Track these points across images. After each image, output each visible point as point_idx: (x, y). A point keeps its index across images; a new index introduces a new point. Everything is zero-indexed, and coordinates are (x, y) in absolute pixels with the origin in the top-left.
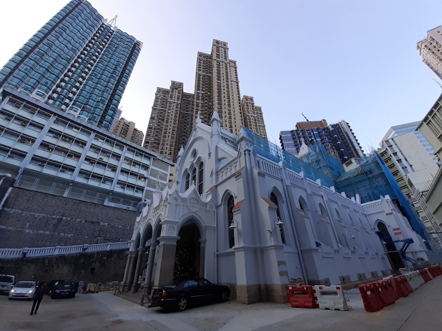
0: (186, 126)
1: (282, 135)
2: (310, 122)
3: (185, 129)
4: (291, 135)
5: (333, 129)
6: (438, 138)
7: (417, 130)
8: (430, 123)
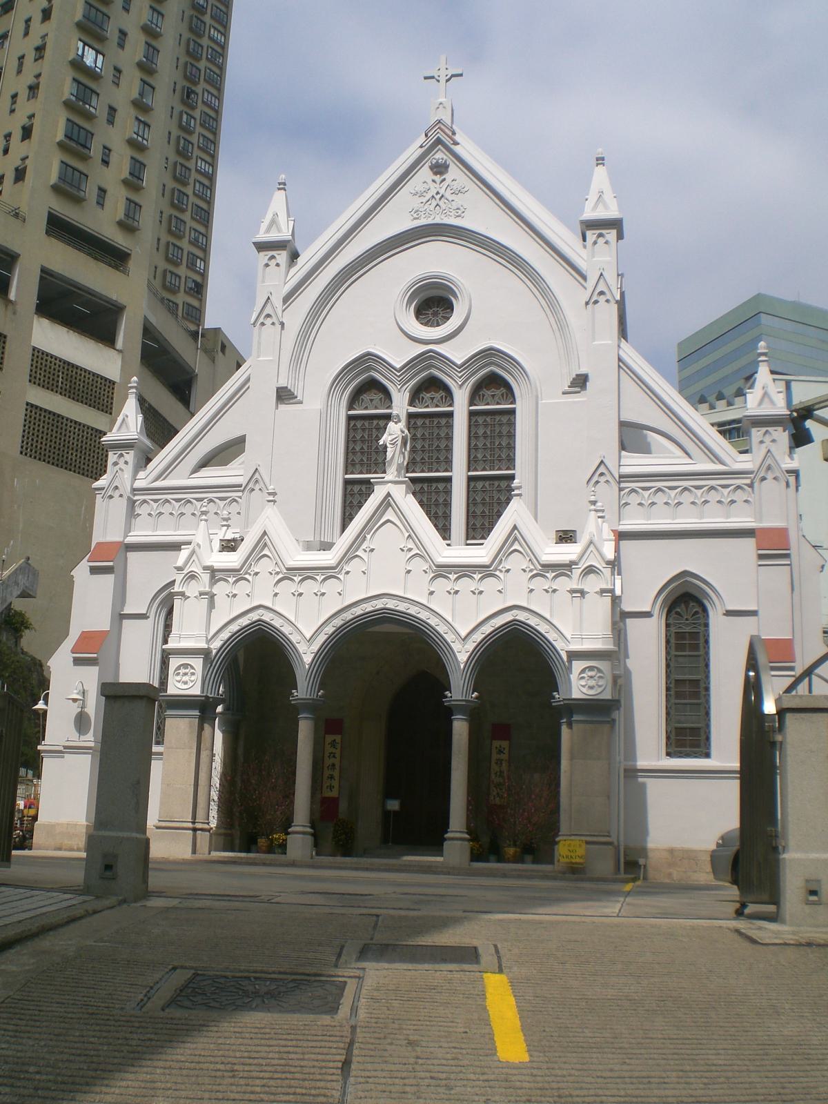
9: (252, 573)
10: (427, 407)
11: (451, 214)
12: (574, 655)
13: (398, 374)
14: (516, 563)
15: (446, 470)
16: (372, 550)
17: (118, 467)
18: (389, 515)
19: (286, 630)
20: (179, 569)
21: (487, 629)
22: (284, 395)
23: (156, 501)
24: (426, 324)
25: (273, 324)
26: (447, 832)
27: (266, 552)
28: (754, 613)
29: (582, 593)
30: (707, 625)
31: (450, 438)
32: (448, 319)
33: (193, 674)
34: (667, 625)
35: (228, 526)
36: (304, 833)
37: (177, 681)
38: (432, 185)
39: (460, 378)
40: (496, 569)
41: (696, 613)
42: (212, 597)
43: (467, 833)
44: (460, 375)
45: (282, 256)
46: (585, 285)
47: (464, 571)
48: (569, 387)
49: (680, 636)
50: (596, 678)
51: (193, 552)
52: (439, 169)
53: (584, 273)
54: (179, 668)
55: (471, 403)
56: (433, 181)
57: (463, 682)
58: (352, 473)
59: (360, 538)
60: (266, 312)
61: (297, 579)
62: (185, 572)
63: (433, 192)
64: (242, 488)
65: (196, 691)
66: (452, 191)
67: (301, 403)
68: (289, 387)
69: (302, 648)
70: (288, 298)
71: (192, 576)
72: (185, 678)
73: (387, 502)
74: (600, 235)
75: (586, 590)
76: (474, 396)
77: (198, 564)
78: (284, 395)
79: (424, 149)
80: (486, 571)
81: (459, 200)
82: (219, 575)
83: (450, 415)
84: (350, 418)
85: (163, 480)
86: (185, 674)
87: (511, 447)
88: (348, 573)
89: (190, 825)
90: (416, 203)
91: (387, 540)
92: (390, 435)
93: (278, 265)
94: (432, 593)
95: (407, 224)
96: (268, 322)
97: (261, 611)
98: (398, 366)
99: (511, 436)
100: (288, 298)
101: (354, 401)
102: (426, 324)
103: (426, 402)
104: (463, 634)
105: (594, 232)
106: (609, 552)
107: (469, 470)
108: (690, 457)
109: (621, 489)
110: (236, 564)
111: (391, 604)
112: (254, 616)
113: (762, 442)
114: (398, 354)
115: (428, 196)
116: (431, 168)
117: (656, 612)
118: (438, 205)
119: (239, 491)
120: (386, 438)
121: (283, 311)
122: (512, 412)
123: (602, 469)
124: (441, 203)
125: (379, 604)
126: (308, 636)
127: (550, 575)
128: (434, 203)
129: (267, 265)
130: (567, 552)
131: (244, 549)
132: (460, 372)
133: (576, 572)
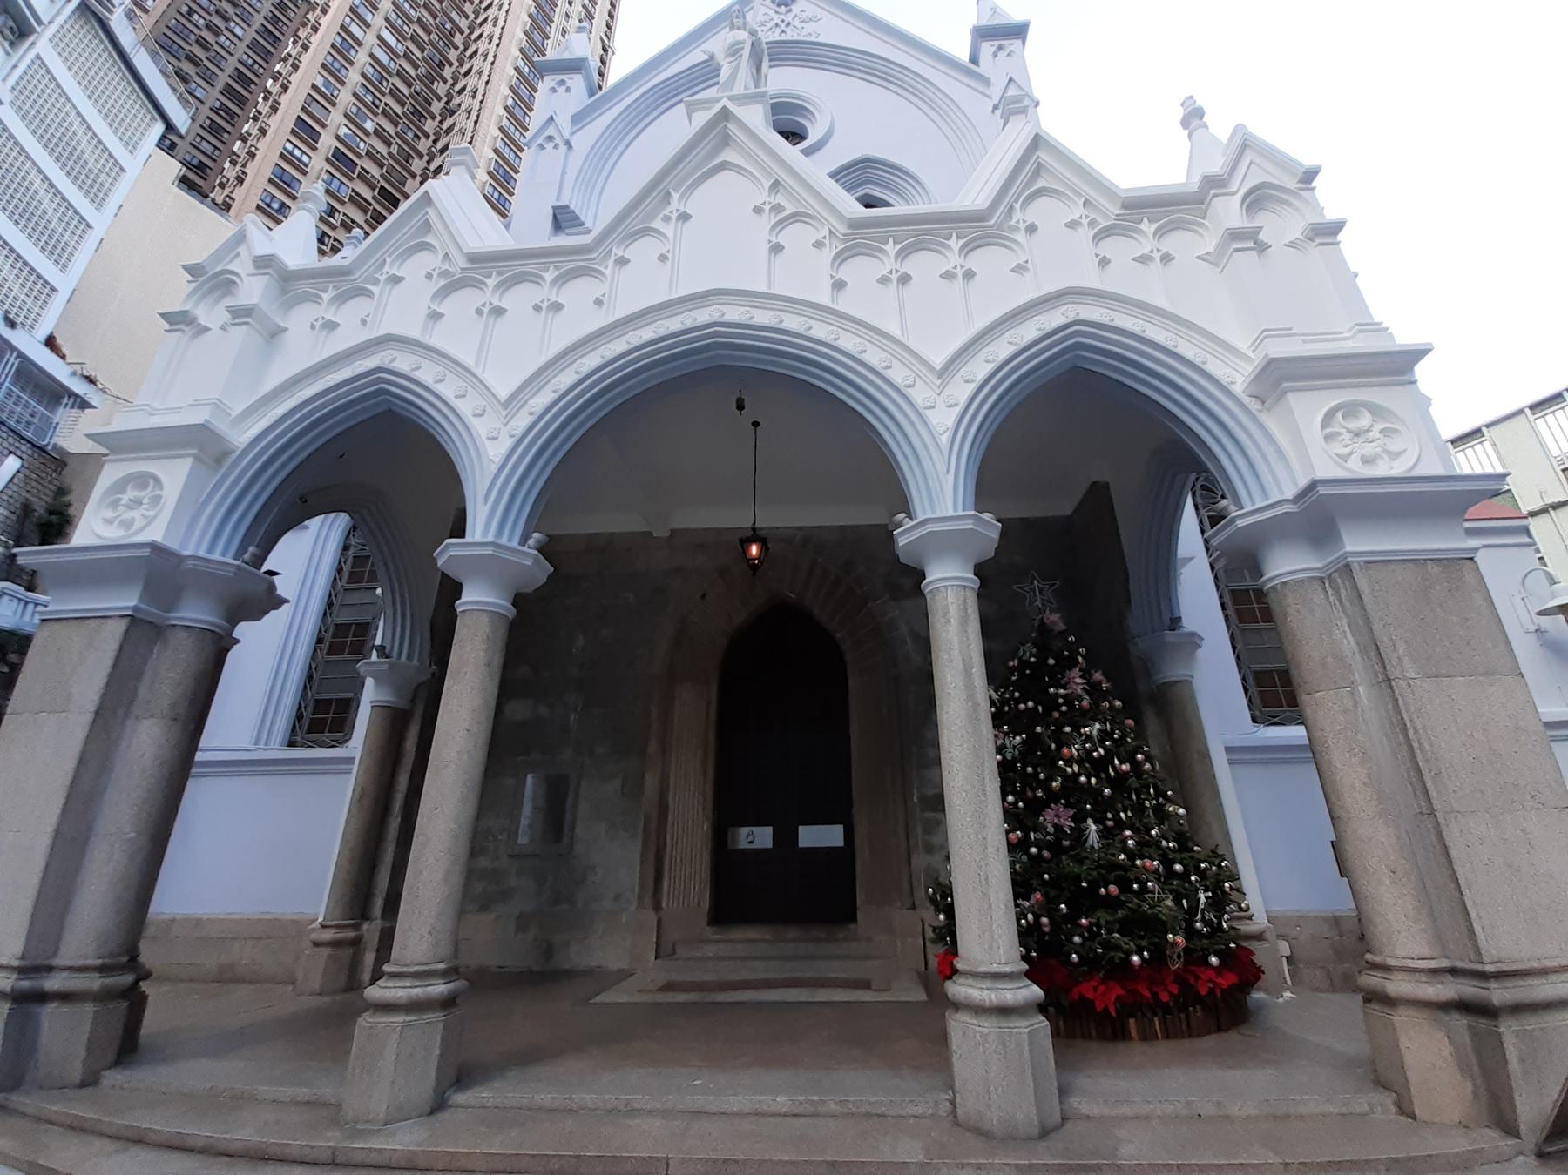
0: (226, 19)
3: (216, 32)
16: (685, 217)
18: (729, 155)
21: (1002, 349)
25: (556, 147)
27: (429, 239)
43: (1031, 975)
45: (577, 82)
50: (1375, 433)
57: (951, 477)
68: (572, 207)
70: (579, 118)
74: (1000, 48)
96: (551, 145)
100: (579, 118)
105: (992, 43)
111: (733, 314)
115: (769, 26)
118: (783, 32)
121: (574, 133)
124: (788, 30)
126: (503, 392)
127: (1148, 228)
129: (554, 90)
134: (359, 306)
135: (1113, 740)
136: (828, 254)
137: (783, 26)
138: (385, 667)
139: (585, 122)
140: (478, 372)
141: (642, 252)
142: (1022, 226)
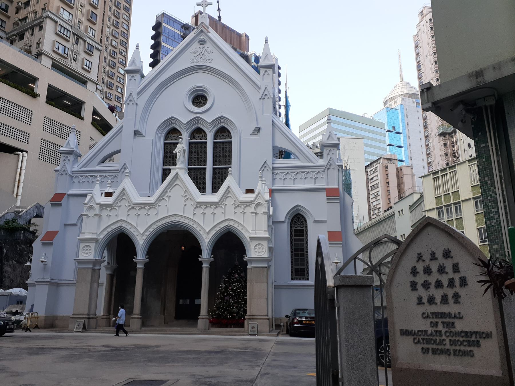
1: (164, 24)
2: (224, 25)
4: (182, 34)
5: (255, 65)
6: (436, 197)
7: (421, 178)
8: (436, 179)
9: (118, 206)
10: (197, 140)
11: (207, 61)
12: (252, 239)
13: (185, 126)
14: (229, 201)
15: (204, 165)
17: (65, 162)
18: (178, 182)
19: (132, 230)
20: (86, 204)
22: (137, 133)
23: (82, 176)
24: (197, 106)
25: (133, 104)
26: (199, 316)
27: (124, 197)
28: (325, 221)
29: (256, 214)
30: (306, 227)
31: (205, 152)
32: (205, 104)
33: (90, 250)
34: (291, 227)
35: (110, 187)
36: (138, 318)
37: (83, 253)
38: (199, 49)
39: (210, 128)
40: (221, 204)
41: (303, 222)
42: (100, 216)
44: (210, 127)
46: (259, 91)
47: (208, 205)
48: (253, 132)
49: (296, 231)
51: (92, 197)
52: (202, 42)
53: (259, 87)
54: (84, 247)
55: (215, 138)
56: (200, 47)
58: (166, 166)
59: (165, 191)
60: (130, 99)
61: (137, 208)
62: (88, 206)
63: (199, 52)
64: (119, 171)
65: (91, 257)
66: (207, 52)
67: (145, 136)
68: (139, 130)
69: (138, 238)
71: (91, 208)
72: (87, 252)
73: (177, 176)
74: (266, 71)
75: (258, 212)
76: (216, 135)
77: (94, 202)
78: (137, 133)
79: (196, 34)
80: (217, 205)
81: (210, 56)
82: (104, 207)
83: (206, 143)
84: (165, 144)
85: (86, 167)
86: (87, 250)
87: (230, 156)
88: (160, 206)
89: (87, 316)
90: (192, 56)
91: (176, 193)
92: (178, 149)
93: (135, 80)
94: (195, 214)
95: (188, 65)
96: (131, 103)
97: (121, 222)
98: (185, 123)
99: (230, 152)
100: (139, 93)
101: (167, 136)
102: (196, 107)
103: (196, 138)
104: (207, 231)
106: (267, 197)
107: (213, 165)
108: (301, 161)
109: (273, 173)
110: (111, 202)
111: (178, 219)
112: (118, 225)
113: (328, 154)
114: (184, 118)
115: (198, 54)
116: (199, 42)
117: (287, 222)
118: (201, 57)
119: (118, 172)
120: (177, 150)
121: (137, 99)
122: (231, 142)
123: (265, 165)
125: (172, 219)
126: (142, 232)
128: (200, 57)
130: (250, 197)
131: (114, 196)
132: (210, 126)
133: (253, 205)
134: (113, 213)
135: (239, 286)
136: (193, 207)
137: (201, 54)
138: (110, 267)
139: (141, 94)
140: (137, 227)
141: (161, 203)
142: (224, 204)
